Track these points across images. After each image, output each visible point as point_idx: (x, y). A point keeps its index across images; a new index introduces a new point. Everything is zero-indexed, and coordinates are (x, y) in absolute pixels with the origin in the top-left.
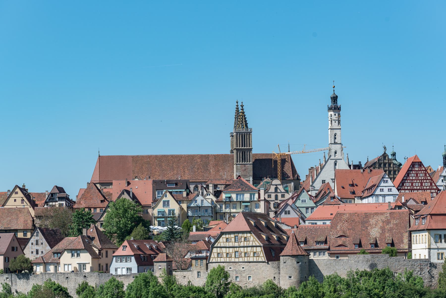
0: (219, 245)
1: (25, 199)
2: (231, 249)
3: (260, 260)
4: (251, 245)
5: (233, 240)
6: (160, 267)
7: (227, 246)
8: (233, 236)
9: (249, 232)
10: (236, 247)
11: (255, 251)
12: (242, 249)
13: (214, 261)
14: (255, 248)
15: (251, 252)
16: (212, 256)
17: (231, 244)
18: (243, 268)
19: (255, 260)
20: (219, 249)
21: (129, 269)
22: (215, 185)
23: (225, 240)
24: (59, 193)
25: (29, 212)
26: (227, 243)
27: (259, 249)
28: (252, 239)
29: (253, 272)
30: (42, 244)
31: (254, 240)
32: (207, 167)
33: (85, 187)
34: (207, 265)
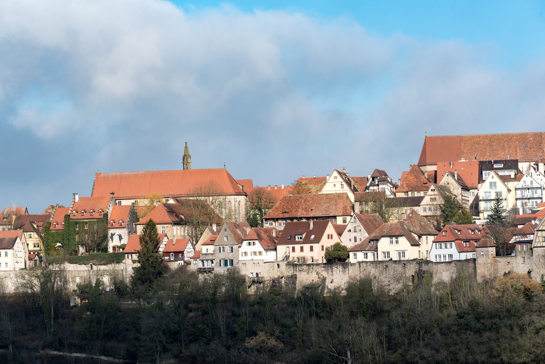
1: (344, 183)
6: (482, 253)
13: (539, 245)
16: (537, 240)
21: (451, 256)
24: (380, 176)
25: (348, 197)
30: (360, 230)
32: (540, 145)
33: (408, 169)
34: (531, 249)
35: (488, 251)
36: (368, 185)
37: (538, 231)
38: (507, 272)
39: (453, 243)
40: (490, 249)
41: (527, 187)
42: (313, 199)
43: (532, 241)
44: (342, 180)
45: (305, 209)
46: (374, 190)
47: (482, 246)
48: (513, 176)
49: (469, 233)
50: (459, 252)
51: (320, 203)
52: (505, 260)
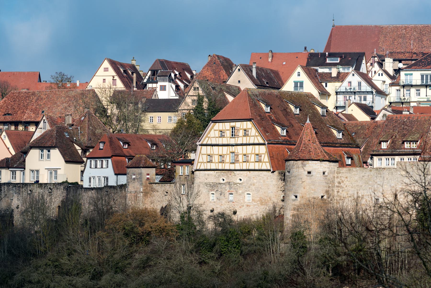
0: (209, 142)
1: (117, 78)
2: (225, 148)
3: (264, 167)
4: (251, 142)
5: (228, 134)
6: (134, 177)
7: (220, 143)
8: (227, 126)
9: (250, 120)
10: (232, 145)
11: (257, 152)
12: (239, 149)
14: (257, 147)
15: (251, 154)
16: (201, 160)
17: (225, 141)
18: (241, 180)
19: (257, 168)
20: (209, 147)
22: (394, 60)
23: (217, 134)
26: (221, 139)
27: (263, 149)
28: (253, 131)
29: (253, 187)
31: (257, 134)
34: (193, 172)
35: (141, 174)
36: (145, 81)
37: (202, 145)
38: (164, 207)
39: (110, 160)
40: (144, 171)
41: (352, 90)
42: (48, 97)
43: (194, 160)
44: (114, 74)
45: (35, 111)
46: (152, 88)
47: (134, 166)
48: (334, 74)
49: (147, 147)
50: (116, 174)
51: (56, 103)
52: (163, 188)
